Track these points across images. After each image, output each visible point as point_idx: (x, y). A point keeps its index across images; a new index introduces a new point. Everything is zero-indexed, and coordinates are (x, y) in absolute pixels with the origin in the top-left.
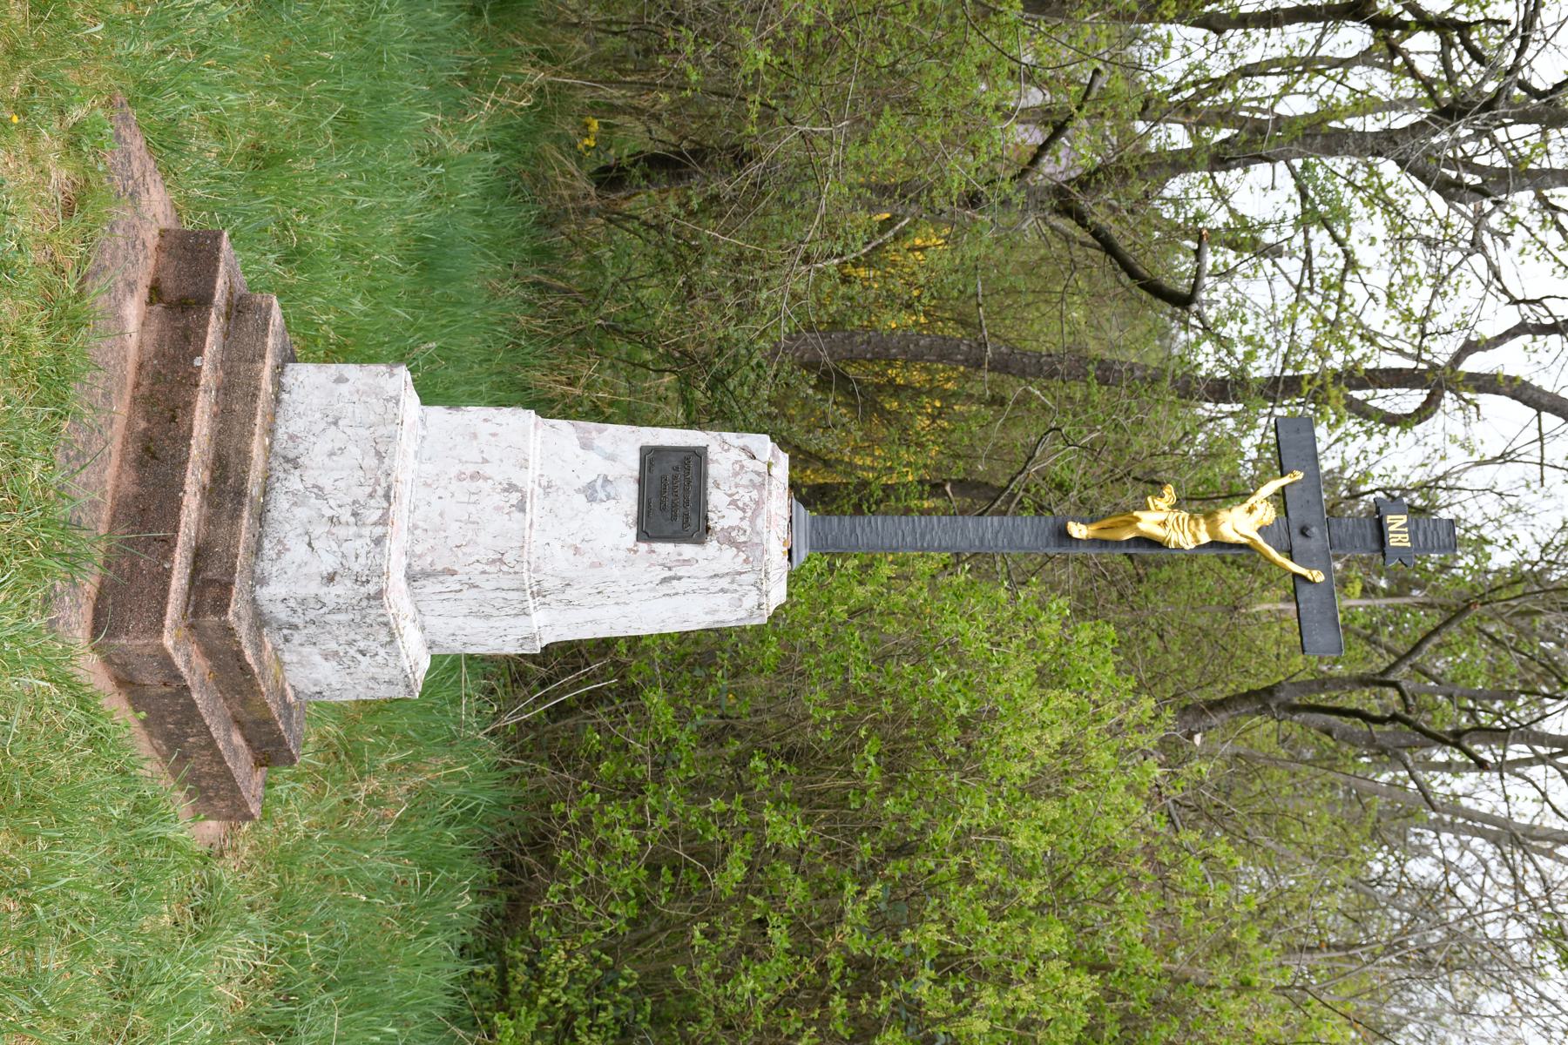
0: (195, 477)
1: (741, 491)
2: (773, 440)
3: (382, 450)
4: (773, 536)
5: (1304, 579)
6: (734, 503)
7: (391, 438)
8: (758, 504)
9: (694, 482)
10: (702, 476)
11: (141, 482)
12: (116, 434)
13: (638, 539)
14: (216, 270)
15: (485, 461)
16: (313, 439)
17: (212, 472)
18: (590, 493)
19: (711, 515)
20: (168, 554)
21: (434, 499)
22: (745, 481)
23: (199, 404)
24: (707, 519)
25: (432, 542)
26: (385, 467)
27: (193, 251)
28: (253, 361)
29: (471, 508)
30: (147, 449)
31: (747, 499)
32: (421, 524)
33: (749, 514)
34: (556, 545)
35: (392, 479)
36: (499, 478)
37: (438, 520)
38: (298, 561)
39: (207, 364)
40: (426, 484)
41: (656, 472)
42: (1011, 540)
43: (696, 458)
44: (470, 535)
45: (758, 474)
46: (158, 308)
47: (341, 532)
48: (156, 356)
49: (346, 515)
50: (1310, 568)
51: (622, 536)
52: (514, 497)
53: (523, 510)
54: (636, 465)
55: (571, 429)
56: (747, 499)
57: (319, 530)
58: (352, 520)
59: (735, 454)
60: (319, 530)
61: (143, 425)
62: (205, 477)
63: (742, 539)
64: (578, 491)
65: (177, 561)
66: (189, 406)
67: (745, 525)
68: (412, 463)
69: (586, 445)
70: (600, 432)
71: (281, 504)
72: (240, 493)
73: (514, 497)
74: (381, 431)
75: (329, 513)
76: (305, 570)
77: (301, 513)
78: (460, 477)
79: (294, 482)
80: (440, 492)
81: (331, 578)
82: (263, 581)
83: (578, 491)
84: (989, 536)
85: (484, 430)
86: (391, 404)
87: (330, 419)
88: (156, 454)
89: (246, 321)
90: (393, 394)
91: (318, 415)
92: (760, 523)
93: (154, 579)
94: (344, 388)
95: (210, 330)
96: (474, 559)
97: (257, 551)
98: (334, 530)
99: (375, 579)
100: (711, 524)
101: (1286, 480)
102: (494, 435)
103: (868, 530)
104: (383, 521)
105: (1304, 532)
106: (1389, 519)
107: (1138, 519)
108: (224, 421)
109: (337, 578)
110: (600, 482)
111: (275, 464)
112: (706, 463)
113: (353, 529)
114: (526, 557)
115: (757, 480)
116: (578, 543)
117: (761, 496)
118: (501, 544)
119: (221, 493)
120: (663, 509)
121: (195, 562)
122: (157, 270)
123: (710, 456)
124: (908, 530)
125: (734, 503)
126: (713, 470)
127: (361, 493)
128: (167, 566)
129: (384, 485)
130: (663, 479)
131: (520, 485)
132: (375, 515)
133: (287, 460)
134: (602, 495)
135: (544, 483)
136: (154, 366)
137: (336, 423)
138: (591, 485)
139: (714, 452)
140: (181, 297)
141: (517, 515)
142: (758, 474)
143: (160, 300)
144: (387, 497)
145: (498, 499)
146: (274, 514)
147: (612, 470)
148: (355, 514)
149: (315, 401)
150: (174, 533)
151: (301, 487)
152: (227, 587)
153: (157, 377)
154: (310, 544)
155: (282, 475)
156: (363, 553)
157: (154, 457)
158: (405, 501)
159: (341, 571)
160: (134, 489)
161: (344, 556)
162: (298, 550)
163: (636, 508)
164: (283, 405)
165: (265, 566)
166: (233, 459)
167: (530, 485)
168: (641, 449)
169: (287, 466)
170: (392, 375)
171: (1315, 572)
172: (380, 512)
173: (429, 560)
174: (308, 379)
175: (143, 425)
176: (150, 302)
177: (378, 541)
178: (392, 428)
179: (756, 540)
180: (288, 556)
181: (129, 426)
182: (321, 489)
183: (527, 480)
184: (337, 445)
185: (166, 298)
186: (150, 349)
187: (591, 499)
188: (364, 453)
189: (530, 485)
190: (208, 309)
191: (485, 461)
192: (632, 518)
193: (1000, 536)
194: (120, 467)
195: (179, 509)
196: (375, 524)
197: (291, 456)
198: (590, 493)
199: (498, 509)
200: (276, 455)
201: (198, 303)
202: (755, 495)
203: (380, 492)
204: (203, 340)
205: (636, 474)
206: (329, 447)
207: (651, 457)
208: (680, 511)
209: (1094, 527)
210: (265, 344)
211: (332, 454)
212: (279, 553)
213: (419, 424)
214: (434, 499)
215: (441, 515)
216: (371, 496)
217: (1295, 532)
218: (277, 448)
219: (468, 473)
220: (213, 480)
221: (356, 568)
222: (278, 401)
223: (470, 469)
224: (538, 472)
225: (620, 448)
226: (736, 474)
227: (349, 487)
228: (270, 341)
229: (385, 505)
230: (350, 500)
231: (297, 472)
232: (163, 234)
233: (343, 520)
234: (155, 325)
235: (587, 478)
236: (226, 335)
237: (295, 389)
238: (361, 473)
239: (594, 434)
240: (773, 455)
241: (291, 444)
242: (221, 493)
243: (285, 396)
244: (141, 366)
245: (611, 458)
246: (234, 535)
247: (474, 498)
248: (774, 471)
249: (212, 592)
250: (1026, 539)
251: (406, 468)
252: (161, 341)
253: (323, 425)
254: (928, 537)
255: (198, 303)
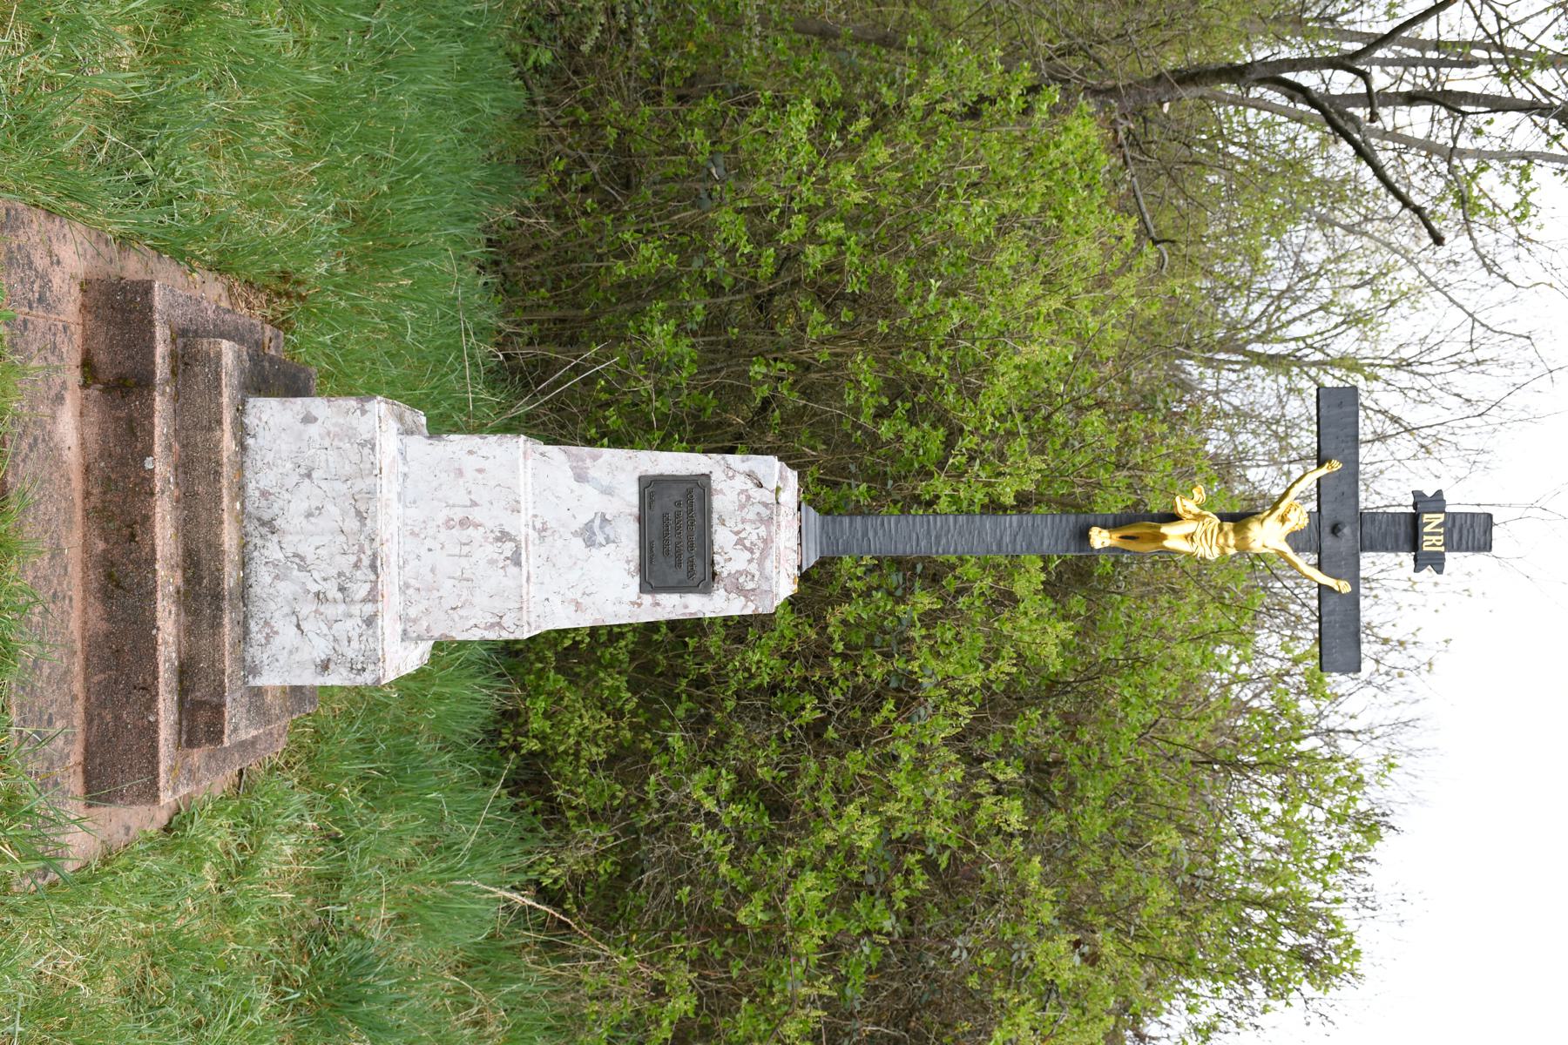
0: (167, 578)
1: (749, 527)
2: (780, 459)
3: (362, 509)
4: (783, 574)
5: (1331, 589)
6: (740, 542)
7: (371, 494)
8: (767, 541)
9: (698, 520)
10: (706, 511)
11: (110, 617)
12: (73, 552)
13: (642, 590)
14: (153, 338)
15: (474, 504)
16: (287, 496)
17: (184, 571)
18: (588, 535)
19: (717, 558)
20: (151, 705)
21: (423, 552)
22: (752, 516)
23: (158, 517)
24: (713, 563)
25: (426, 603)
26: (367, 530)
27: (123, 311)
28: (210, 429)
29: (464, 562)
30: (109, 576)
31: (754, 537)
32: (412, 582)
33: (757, 555)
34: (556, 600)
35: (377, 544)
36: (490, 524)
37: (429, 577)
38: (288, 647)
39: (160, 465)
40: (412, 533)
41: (656, 506)
42: (1029, 545)
43: (699, 487)
44: (465, 593)
45: (766, 505)
46: (94, 392)
47: (330, 610)
48: (101, 456)
49: (333, 593)
50: (1337, 578)
51: (625, 586)
52: (509, 548)
53: (518, 564)
54: (635, 499)
55: (563, 457)
56: (754, 537)
57: (306, 609)
58: (339, 596)
59: (741, 483)
60: (306, 609)
61: (101, 546)
62: (178, 579)
63: (750, 586)
64: (575, 534)
65: (161, 713)
66: (147, 520)
67: (753, 568)
68: (396, 509)
69: (581, 477)
70: (595, 458)
71: (262, 577)
72: (217, 597)
73: (509, 548)
74: (360, 485)
75: (314, 588)
76: (297, 657)
77: (286, 588)
78: (449, 523)
79: (273, 552)
80: (429, 543)
81: (325, 666)
82: (254, 671)
83: (575, 534)
84: (1007, 539)
85: (470, 464)
86: (366, 451)
87: (303, 471)
88: (120, 581)
89: (196, 375)
90: (367, 436)
91: (289, 465)
92: (769, 565)
93: (141, 735)
94: (313, 430)
95: (156, 420)
96: (472, 623)
97: (245, 636)
98: (322, 609)
99: (371, 667)
100: (717, 568)
101: (1324, 471)
102: (480, 471)
103: (880, 533)
104: (372, 597)
105: (1335, 529)
106: (1426, 517)
107: (1164, 537)
108: (188, 507)
109: (332, 666)
110: (597, 522)
111: (250, 528)
112: (710, 495)
113: (342, 608)
114: (525, 618)
115: (765, 512)
116: (578, 596)
117: (769, 532)
118: (498, 605)
119: (196, 597)
120: (666, 553)
121: (181, 682)
122: (86, 339)
123: (714, 485)
124: (922, 532)
125: (740, 542)
126: (719, 503)
127: (346, 563)
128: (152, 719)
129: (369, 552)
130: (665, 516)
131: (513, 533)
132: (362, 590)
133: (263, 524)
134: (600, 538)
135: (538, 525)
136: (101, 469)
137: (309, 476)
138: (588, 527)
139: (718, 481)
140: (118, 383)
141: (512, 570)
142: (766, 505)
143: (96, 380)
144: (373, 567)
145: (491, 550)
146: (256, 590)
147: (611, 507)
148: (342, 589)
149: (284, 447)
150: (151, 644)
151: (280, 556)
152: (218, 709)
153: (107, 482)
154: (298, 626)
155: (259, 542)
156: (354, 635)
157: (118, 586)
158: (393, 559)
159: (334, 657)
160: (104, 626)
161: (335, 640)
162: (287, 633)
163: (637, 552)
164: (250, 453)
165: (254, 652)
166: (204, 555)
167: (523, 530)
168: (640, 479)
169: (264, 530)
170: (364, 412)
171: (1342, 583)
172: (367, 586)
173: (425, 624)
174: (270, 413)
175: (101, 546)
176: (85, 386)
177: (370, 621)
178: (370, 480)
179: (765, 587)
180: (277, 641)
181: (87, 547)
182: (302, 559)
183: (519, 526)
184: (315, 503)
185: (101, 376)
186: (94, 447)
187: (590, 543)
188: (344, 513)
189: (523, 530)
190: (151, 392)
191: (474, 504)
192: (634, 565)
193: (1019, 538)
194: (84, 599)
195: (155, 650)
196: (364, 601)
197: (266, 517)
198: (588, 535)
199: (492, 562)
200: (249, 516)
201: (138, 384)
202: (763, 531)
203: (366, 562)
204: (151, 434)
205: (636, 510)
206: (305, 506)
207: (651, 487)
208: (685, 556)
209: (1116, 535)
210: (219, 405)
211: (309, 515)
212: (268, 637)
213: (399, 458)
214: (423, 552)
215: (433, 570)
216: (356, 566)
217: (1326, 530)
218: (250, 508)
219: (457, 519)
220: (187, 581)
221: (350, 654)
222: (243, 447)
223: (458, 514)
224: (531, 512)
225: (618, 474)
226: (742, 507)
227: (332, 556)
228: (225, 400)
229: (373, 577)
230: (334, 572)
231: (275, 538)
232: (86, 286)
233: (330, 596)
234: (94, 415)
235: (583, 519)
236: (176, 397)
237: (260, 430)
238: (343, 538)
239: (588, 462)
240: (781, 478)
241: (264, 503)
242: (196, 597)
243: (250, 441)
244: (87, 470)
245: (608, 491)
246: (218, 647)
247: (466, 549)
248: (783, 497)
249: (203, 716)
250: (1046, 542)
251: (390, 521)
252: (104, 433)
253: (295, 478)
254: (943, 541)
255: (138, 384)
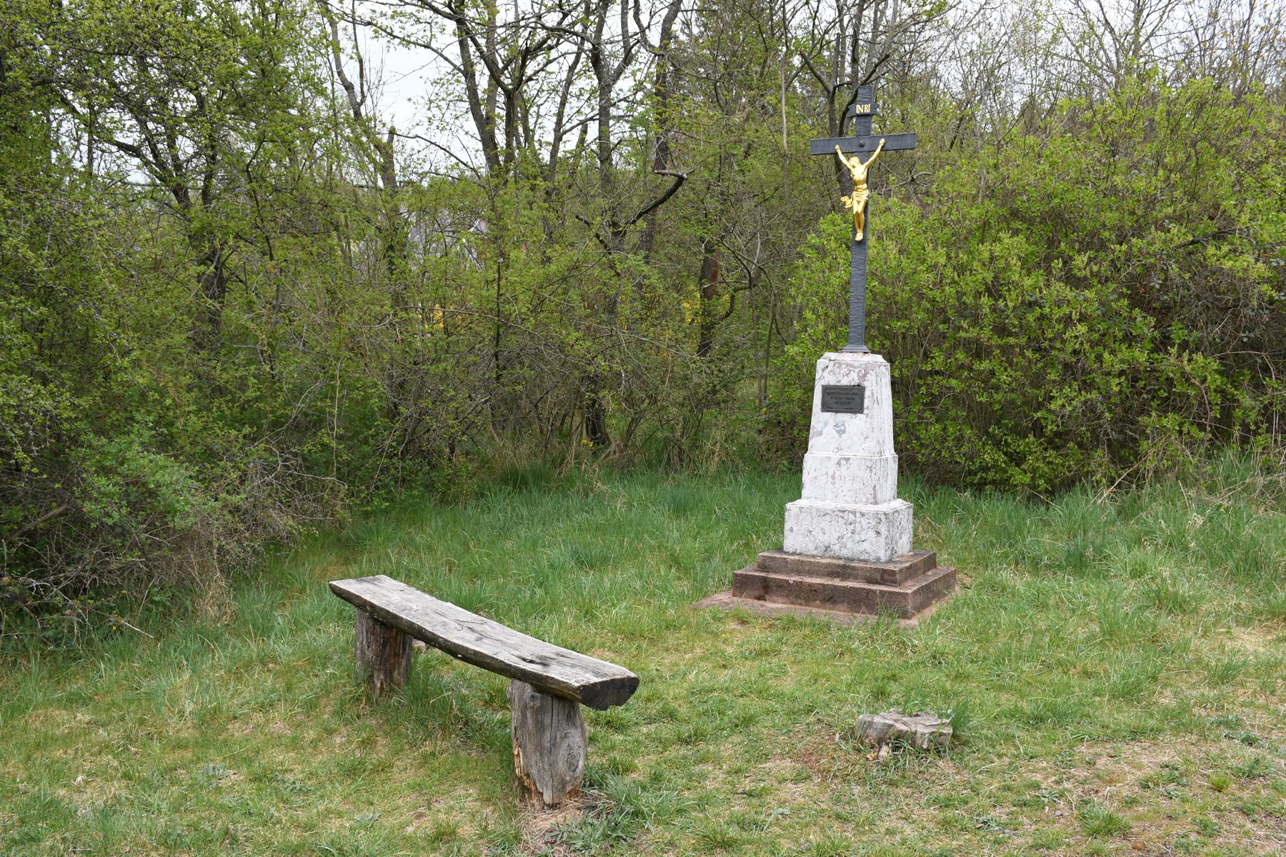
0: (837, 582)
7: (818, 510)
8: (847, 365)
10: (835, 387)
20: (874, 592)
39: (792, 579)
43: (827, 390)
47: (858, 529)
52: (843, 462)
57: (857, 538)
59: (826, 374)
60: (857, 538)
66: (810, 585)
68: (826, 502)
69: (820, 433)
71: (845, 553)
72: (844, 567)
73: (843, 462)
77: (849, 545)
79: (836, 548)
81: (878, 533)
82: (878, 559)
85: (812, 474)
88: (831, 597)
97: (865, 561)
105: (862, 146)
118: (863, 467)
126: (833, 383)
127: (841, 522)
139: (825, 382)
140: (764, 588)
145: (843, 469)
152: (884, 571)
153: (797, 597)
162: (866, 546)
177: (863, 515)
181: (818, 607)
187: (844, 432)
207: (826, 407)
223: (830, 480)
225: (821, 420)
232: (734, 595)
234: (775, 598)
245: (826, 424)
246: (862, 569)
249: (886, 577)
251: (829, 505)
